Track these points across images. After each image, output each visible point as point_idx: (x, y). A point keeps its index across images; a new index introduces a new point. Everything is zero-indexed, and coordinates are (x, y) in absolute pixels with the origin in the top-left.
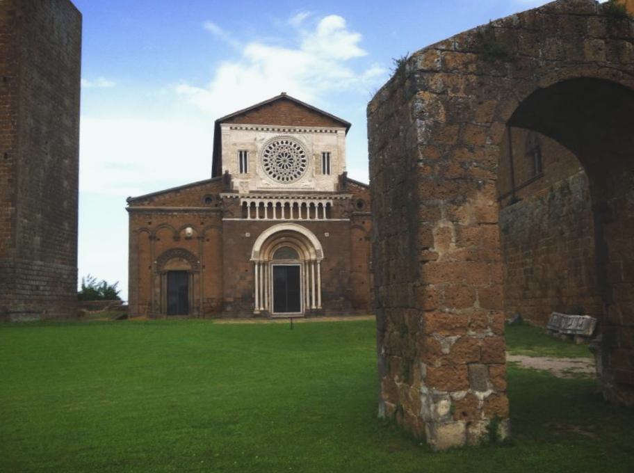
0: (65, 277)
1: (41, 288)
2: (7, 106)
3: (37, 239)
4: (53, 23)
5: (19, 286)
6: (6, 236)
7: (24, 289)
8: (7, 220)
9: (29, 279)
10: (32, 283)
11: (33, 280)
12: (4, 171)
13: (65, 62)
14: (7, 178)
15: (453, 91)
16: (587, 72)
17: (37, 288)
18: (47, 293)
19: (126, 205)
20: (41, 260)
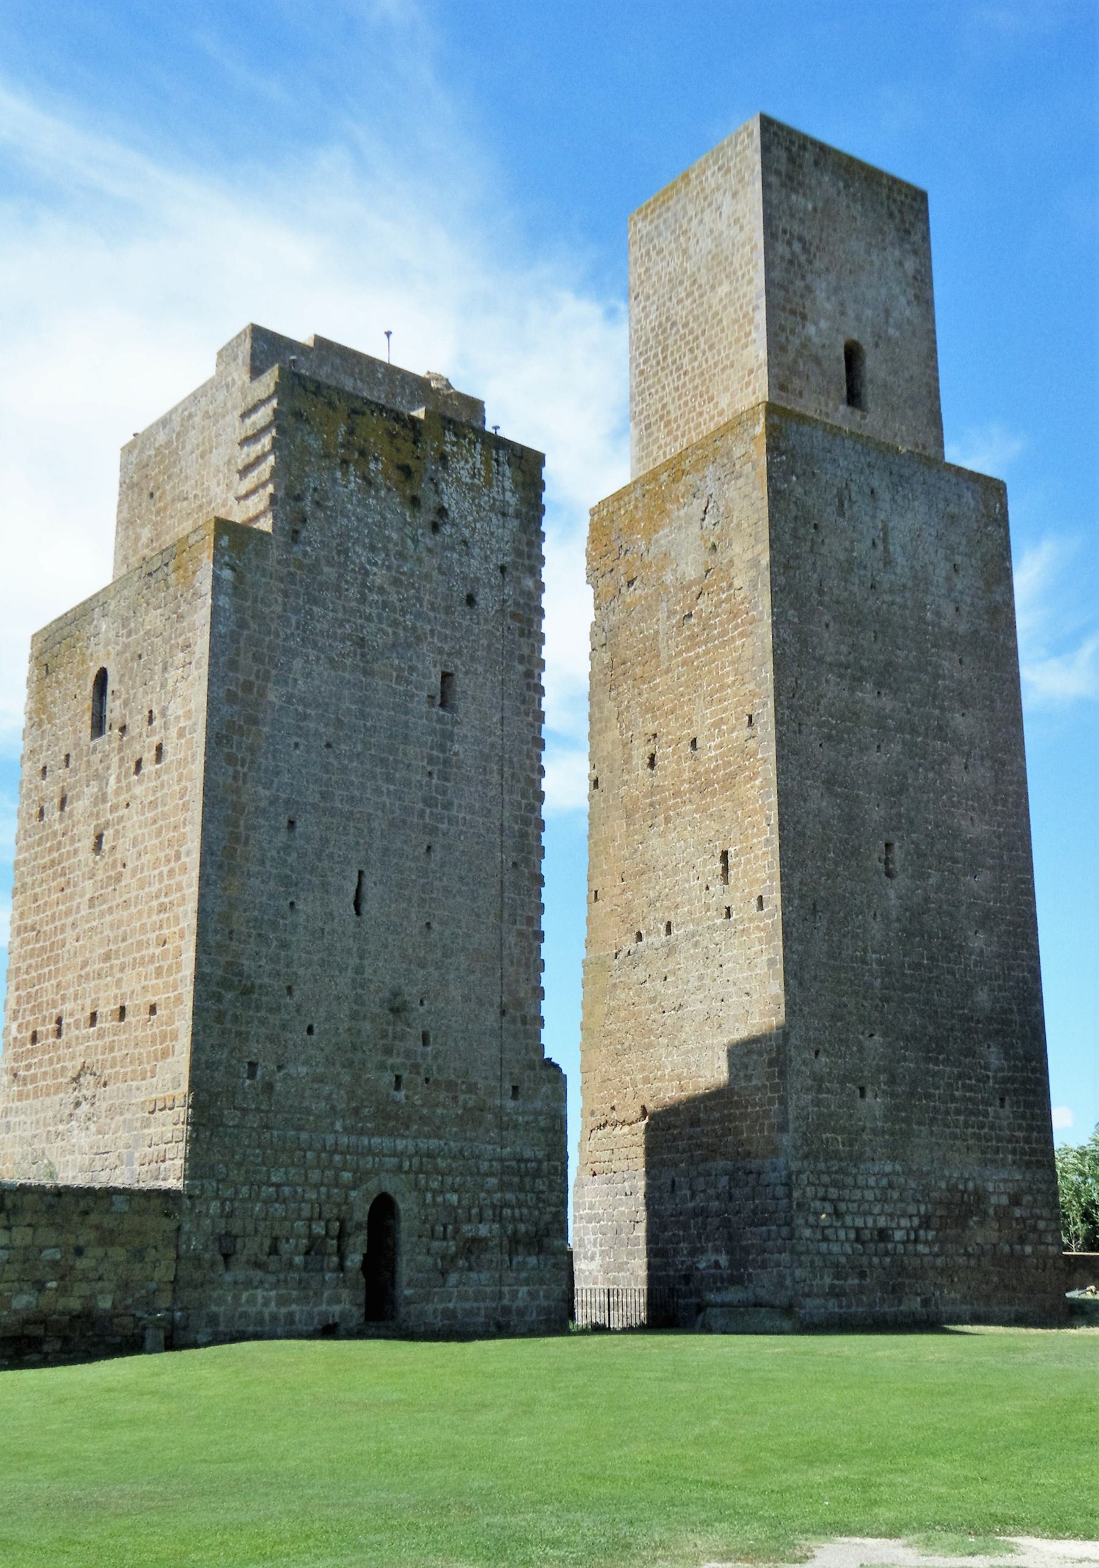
0: (1004, 1200)
1: (899, 1235)
2: (757, 782)
3: (874, 1104)
4: (885, 541)
5: (807, 1233)
6: (771, 1101)
7: (825, 1239)
8: (771, 1063)
9: (848, 1212)
10: (859, 1222)
11: (866, 1214)
12: (760, 940)
13: (945, 624)
14: (765, 957)
17: (883, 1235)
18: (921, 1248)
20: (894, 1159)
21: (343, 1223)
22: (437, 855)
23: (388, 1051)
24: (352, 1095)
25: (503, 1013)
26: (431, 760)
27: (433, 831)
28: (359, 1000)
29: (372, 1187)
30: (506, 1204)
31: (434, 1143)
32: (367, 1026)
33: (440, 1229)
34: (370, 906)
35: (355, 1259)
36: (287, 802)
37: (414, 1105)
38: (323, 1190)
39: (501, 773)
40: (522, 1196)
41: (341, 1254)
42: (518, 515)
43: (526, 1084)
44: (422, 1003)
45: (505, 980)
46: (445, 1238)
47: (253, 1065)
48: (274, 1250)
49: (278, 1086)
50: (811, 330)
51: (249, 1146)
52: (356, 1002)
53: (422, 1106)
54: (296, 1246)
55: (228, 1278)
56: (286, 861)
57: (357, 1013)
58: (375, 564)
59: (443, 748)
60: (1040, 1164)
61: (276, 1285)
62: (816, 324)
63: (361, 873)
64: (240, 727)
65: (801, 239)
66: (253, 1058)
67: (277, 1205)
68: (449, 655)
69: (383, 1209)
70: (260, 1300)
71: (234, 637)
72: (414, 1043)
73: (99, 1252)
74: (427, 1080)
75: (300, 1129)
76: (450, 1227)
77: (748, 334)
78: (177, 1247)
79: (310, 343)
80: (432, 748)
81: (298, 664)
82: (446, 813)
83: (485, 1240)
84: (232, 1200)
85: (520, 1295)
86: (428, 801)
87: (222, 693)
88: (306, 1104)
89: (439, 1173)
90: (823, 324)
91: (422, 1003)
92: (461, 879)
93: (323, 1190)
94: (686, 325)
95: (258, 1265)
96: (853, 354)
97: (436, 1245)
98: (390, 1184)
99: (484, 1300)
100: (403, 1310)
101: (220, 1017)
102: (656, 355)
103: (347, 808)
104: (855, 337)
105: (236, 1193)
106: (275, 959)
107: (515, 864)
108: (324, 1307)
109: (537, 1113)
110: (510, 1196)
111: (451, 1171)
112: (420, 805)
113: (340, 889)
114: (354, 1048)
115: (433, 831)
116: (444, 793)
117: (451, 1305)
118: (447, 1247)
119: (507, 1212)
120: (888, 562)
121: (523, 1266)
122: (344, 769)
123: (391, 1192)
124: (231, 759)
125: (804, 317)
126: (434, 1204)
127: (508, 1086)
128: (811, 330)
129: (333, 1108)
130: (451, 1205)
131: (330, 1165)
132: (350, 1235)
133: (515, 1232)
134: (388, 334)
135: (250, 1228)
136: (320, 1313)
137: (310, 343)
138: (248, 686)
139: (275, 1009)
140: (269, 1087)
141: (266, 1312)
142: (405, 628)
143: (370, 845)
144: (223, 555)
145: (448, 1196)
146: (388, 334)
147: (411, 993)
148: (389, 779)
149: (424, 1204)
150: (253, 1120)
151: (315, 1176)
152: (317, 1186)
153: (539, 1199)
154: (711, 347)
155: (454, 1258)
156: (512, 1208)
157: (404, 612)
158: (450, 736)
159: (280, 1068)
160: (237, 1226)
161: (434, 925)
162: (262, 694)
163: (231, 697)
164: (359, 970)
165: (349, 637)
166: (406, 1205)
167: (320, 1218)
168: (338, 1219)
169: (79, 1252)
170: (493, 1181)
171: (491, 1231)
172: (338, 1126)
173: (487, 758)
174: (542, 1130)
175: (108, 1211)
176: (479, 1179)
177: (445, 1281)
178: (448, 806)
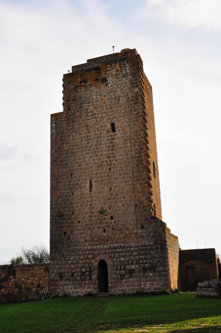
21: (90, 268)
22: (112, 170)
23: (101, 223)
24: (91, 236)
25: (136, 206)
26: (108, 147)
27: (111, 164)
28: (92, 212)
29: (98, 258)
30: (141, 259)
31: (116, 245)
32: (94, 218)
33: (119, 267)
36: (70, 170)
37: (109, 236)
38: (84, 260)
39: (131, 143)
40: (146, 256)
42: (131, 74)
43: (146, 225)
44: (110, 209)
45: (136, 198)
46: (121, 270)
47: (65, 233)
48: (72, 276)
49: (71, 237)
51: (64, 252)
52: (91, 213)
53: (112, 236)
54: (78, 275)
55: (61, 283)
56: (70, 184)
57: (91, 215)
58: (90, 106)
59: (112, 143)
61: (73, 285)
63: (91, 181)
64: (58, 157)
66: (65, 231)
67: (72, 265)
68: (112, 119)
69: (103, 265)
70: (69, 288)
71: (56, 138)
72: (108, 220)
73: (33, 278)
74: (113, 229)
75: (78, 246)
76: (122, 267)
78: (49, 276)
79: (86, 62)
80: (109, 144)
81: (71, 138)
82: (114, 159)
83: (134, 270)
84: (61, 265)
85: (147, 285)
86: (109, 157)
87: (53, 151)
88: (79, 240)
89: (118, 253)
91: (110, 209)
92: (120, 174)
93: (84, 260)
97: (118, 272)
98: (103, 257)
99: (135, 286)
100: (109, 289)
101: (56, 223)
103: (85, 167)
105: (62, 263)
106: (69, 207)
107: (137, 165)
108: (86, 289)
109: (150, 232)
110: (142, 257)
111: (121, 252)
112: (106, 159)
113: (85, 187)
114: (91, 224)
115: (111, 164)
116: (113, 154)
117: (124, 288)
118: (122, 272)
119: (141, 261)
121: (148, 276)
122: (84, 158)
123: (103, 259)
124: (56, 165)
126: (117, 261)
127: (139, 226)
129: (86, 240)
130: (122, 261)
131: (86, 254)
132: (92, 271)
133: (144, 266)
134: (113, 47)
135: (66, 271)
136: (85, 291)
137: (86, 62)
138: (59, 148)
139: (69, 219)
140: (69, 238)
141: (71, 291)
142: (99, 118)
143: (92, 174)
144: (52, 122)
145: (121, 259)
146: (113, 47)
147: (106, 208)
148: (96, 156)
149: (114, 262)
150: (65, 246)
151: (82, 257)
152: (82, 260)
153: (152, 257)
155: (124, 275)
156: (143, 260)
157: (98, 114)
158: (114, 139)
159: (72, 232)
160: (62, 271)
161: (113, 189)
162: (63, 148)
163: (56, 151)
164: (91, 205)
165: (84, 126)
166: (109, 263)
167: (84, 267)
168: (89, 267)
169: (28, 279)
170: (136, 253)
171: (136, 267)
172: (87, 245)
173: (126, 140)
174: (152, 237)
175: (34, 269)
176: (131, 253)
177: (122, 281)
178: (114, 157)
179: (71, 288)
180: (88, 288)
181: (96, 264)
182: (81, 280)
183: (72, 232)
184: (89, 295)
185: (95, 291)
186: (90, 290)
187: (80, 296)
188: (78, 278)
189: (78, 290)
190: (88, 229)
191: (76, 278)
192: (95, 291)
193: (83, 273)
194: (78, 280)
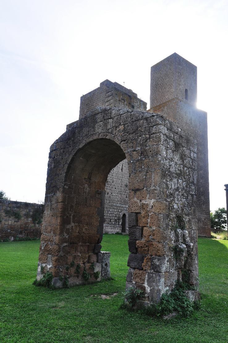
15: (57, 157)
16: (95, 137)
19: (225, 188)
23: (125, 192)
24: (121, 199)
28: (122, 184)
29: (123, 213)
32: (123, 188)
34: (123, 170)
35: (120, 223)
41: (119, 223)
47: (108, 193)
48: (110, 221)
50: (181, 87)
60: (208, 214)
61: (111, 227)
62: (181, 86)
65: (180, 73)
77: (171, 87)
90: (183, 86)
94: (160, 85)
95: (108, 223)
96: (186, 90)
102: (155, 89)
104: (187, 89)
120: (191, 123)
125: (180, 85)
128: (181, 87)
134: (124, 82)
140: (110, 197)
146: (124, 82)
154: (165, 88)
159: (111, 194)
164: (122, 180)
179: (109, 229)
180: (118, 229)
181: (122, 216)
182: (114, 224)
183: (111, 194)
184: (117, 233)
185: (120, 232)
186: (118, 230)
187: (113, 234)
188: (113, 223)
189: (113, 230)
190: (120, 194)
191: (112, 223)
192: (120, 232)
193: (115, 220)
194: (113, 224)
